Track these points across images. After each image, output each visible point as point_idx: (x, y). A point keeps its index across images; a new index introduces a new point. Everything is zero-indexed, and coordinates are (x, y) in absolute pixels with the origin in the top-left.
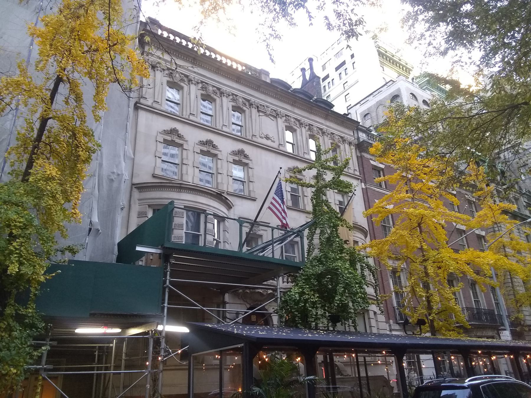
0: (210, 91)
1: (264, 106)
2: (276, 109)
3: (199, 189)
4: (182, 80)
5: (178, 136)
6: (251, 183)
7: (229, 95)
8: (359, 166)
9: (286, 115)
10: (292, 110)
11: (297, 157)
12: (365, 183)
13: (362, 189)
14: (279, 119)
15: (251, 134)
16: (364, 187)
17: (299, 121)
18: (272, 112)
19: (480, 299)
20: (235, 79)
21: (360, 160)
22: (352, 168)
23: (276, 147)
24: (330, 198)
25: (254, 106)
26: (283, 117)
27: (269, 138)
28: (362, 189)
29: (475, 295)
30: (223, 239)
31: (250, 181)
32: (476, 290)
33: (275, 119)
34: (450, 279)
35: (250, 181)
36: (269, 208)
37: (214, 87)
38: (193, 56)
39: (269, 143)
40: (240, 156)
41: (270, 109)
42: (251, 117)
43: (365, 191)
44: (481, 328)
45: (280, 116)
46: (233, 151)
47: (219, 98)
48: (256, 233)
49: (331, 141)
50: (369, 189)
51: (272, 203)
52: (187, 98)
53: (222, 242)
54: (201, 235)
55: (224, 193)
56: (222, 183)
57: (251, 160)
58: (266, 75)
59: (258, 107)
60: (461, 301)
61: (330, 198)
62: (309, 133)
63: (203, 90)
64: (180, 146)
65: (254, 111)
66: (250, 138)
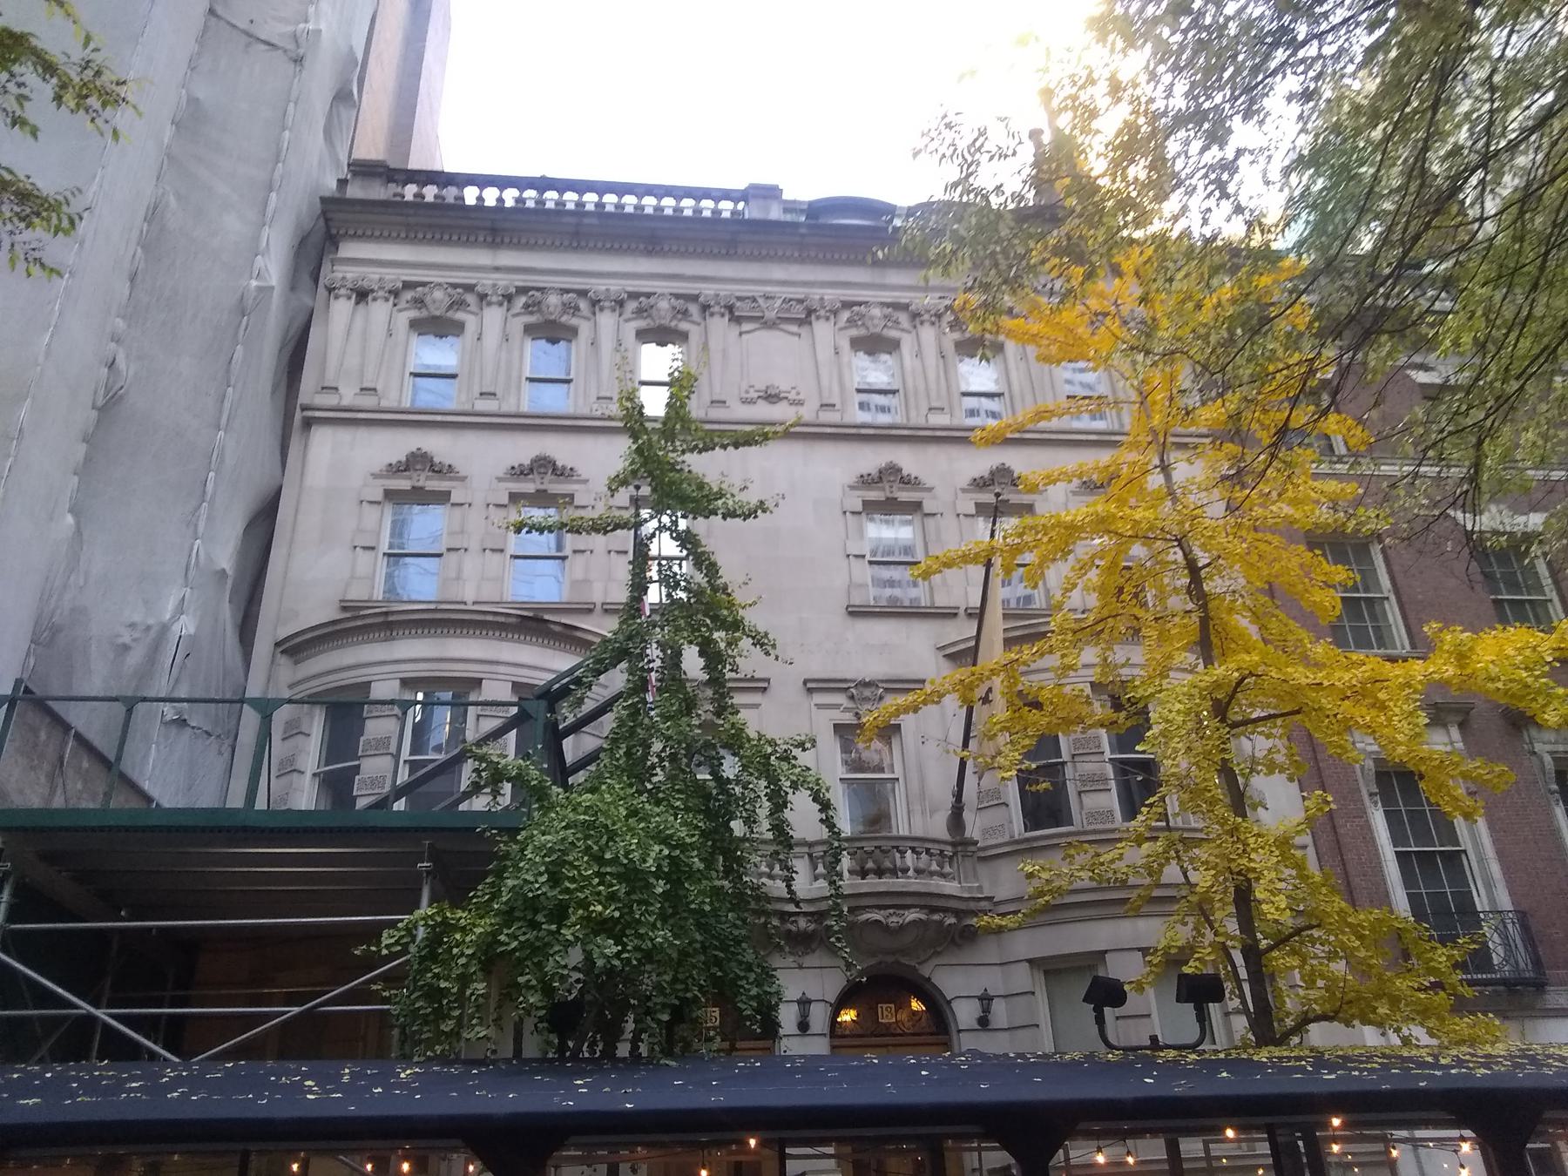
0: (551, 309)
1: (754, 300)
2: (802, 296)
3: (446, 616)
4: (460, 304)
5: (434, 471)
9: (847, 305)
10: (878, 280)
11: (894, 432)
17: (904, 307)
20: (642, 246)
25: (716, 309)
33: (804, 331)
37: (568, 291)
38: (488, 224)
39: (780, 413)
58: (765, 197)
59: (730, 308)
63: (531, 313)
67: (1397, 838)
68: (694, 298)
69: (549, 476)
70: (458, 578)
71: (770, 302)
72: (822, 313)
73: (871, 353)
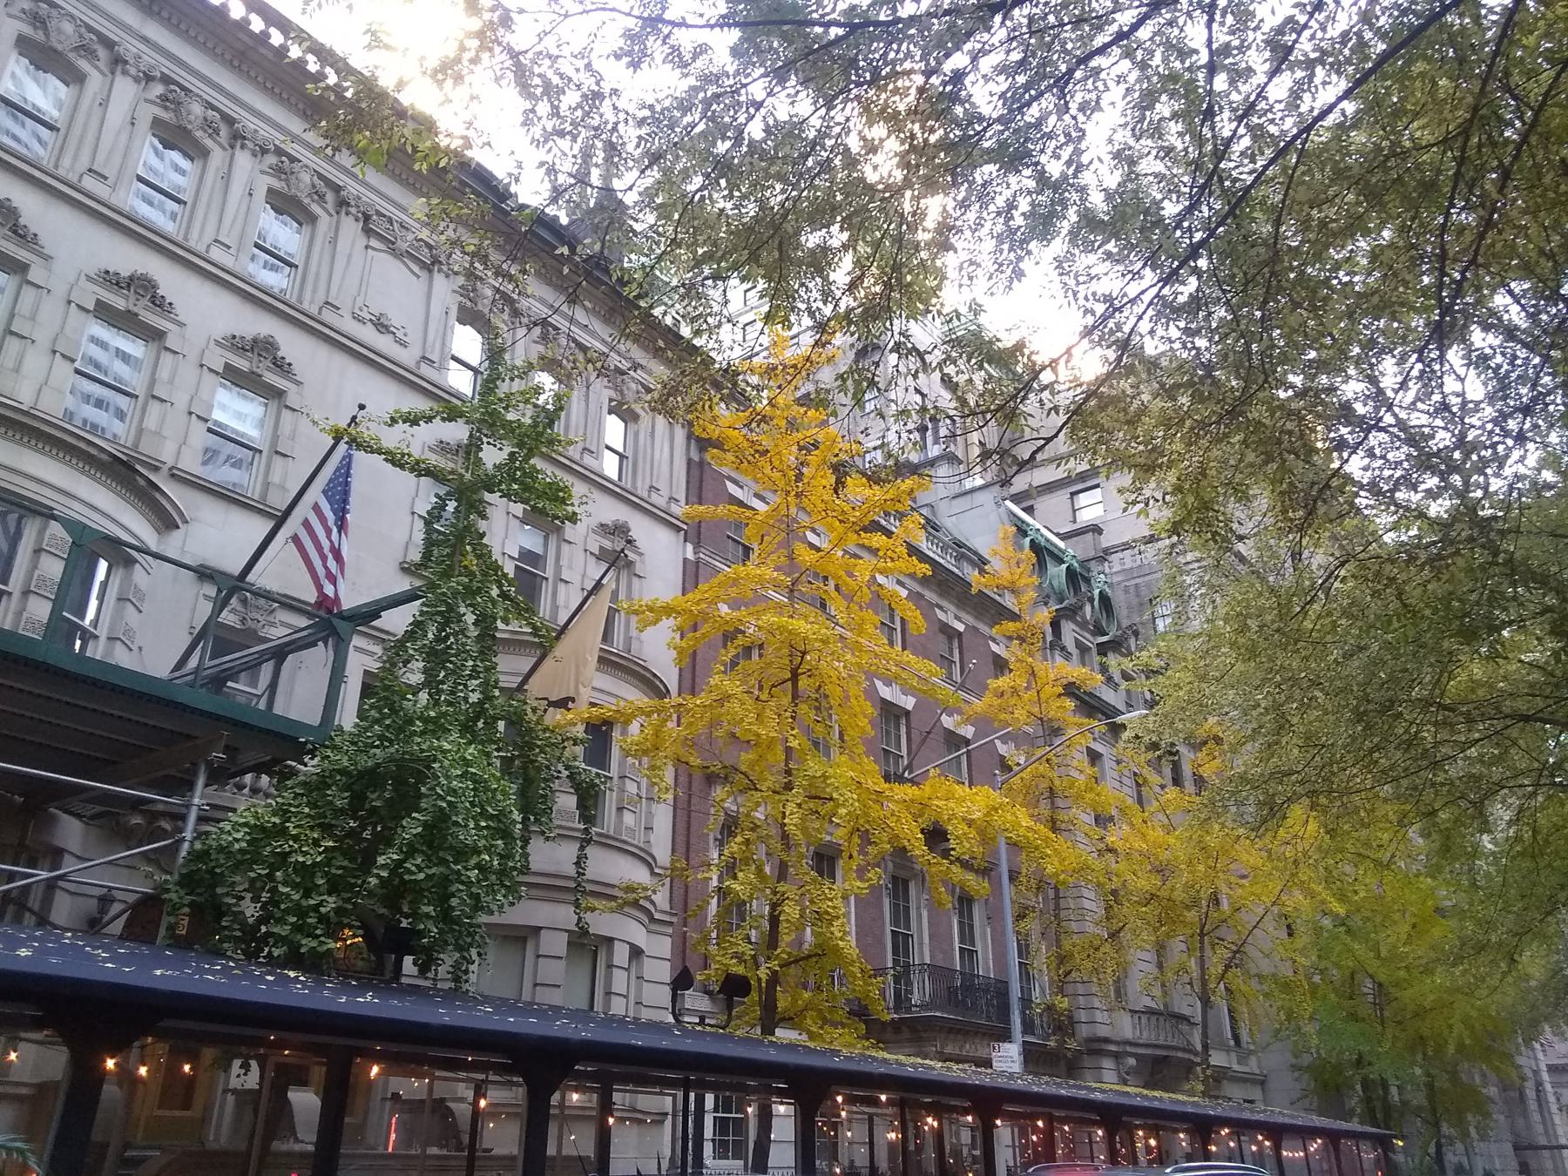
0: (192, 118)
1: (390, 221)
3: (36, 424)
4: (85, 50)
5: (15, 232)
6: (278, 460)
7: (264, 151)
8: (688, 489)
12: (697, 546)
13: (685, 560)
14: (439, 279)
15: (321, 297)
16: (690, 555)
18: (417, 249)
19: (979, 947)
20: (301, 106)
21: (695, 472)
22: (665, 492)
23: (411, 364)
24: (570, 567)
25: (353, 210)
26: (456, 273)
27: (386, 327)
28: (685, 560)
29: (967, 933)
30: (111, 628)
31: (277, 452)
32: (971, 918)
33: (424, 274)
34: (903, 874)
35: (277, 452)
36: (296, 539)
37: (214, 108)
39: (383, 343)
40: (256, 358)
41: (410, 237)
42: (334, 241)
43: (691, 569)
44: (959, 1031)
45: (445, 268)
46: (234, 337)
47: (224, 149)
48: (255, 631)
49: (612, 394)
50: (707, 564)
51: (306, 524)
52: (89, 115)
53: (103, 639)
54: (10, 594)
55: (156, 469)
56: (158, 433)
57: (298, 383)
59: (367, 218)
60: (921, 944)
61: (570, 567)
62: (541, 348)
63: (166, 108)
64: (153, 336)
65: (350, 228)
66: (314, 311)
67: (961, 942)
68: (337, 189)
69: (145, 302)
70: (17, 370)
71: (404, 232)
72: (445, 268)
73: (279, 211)
